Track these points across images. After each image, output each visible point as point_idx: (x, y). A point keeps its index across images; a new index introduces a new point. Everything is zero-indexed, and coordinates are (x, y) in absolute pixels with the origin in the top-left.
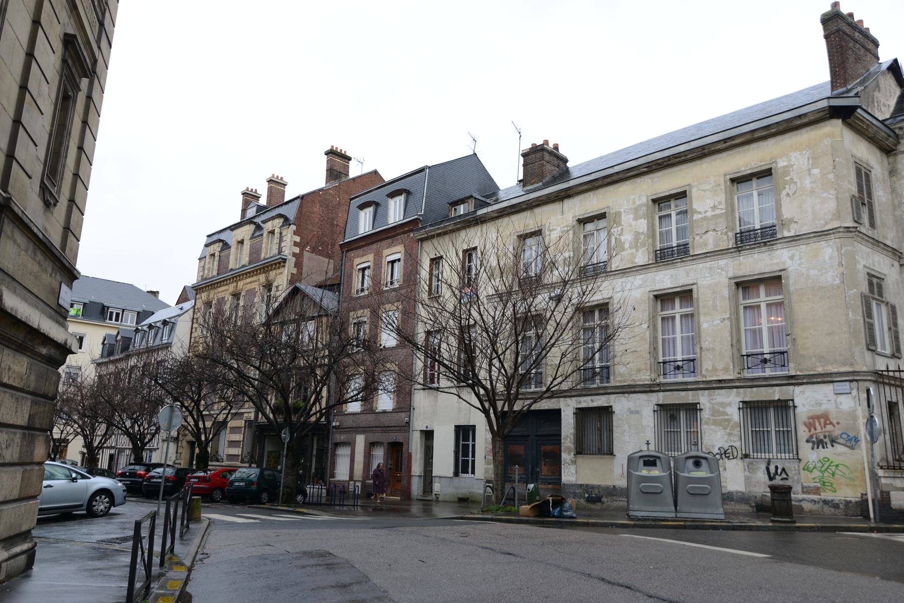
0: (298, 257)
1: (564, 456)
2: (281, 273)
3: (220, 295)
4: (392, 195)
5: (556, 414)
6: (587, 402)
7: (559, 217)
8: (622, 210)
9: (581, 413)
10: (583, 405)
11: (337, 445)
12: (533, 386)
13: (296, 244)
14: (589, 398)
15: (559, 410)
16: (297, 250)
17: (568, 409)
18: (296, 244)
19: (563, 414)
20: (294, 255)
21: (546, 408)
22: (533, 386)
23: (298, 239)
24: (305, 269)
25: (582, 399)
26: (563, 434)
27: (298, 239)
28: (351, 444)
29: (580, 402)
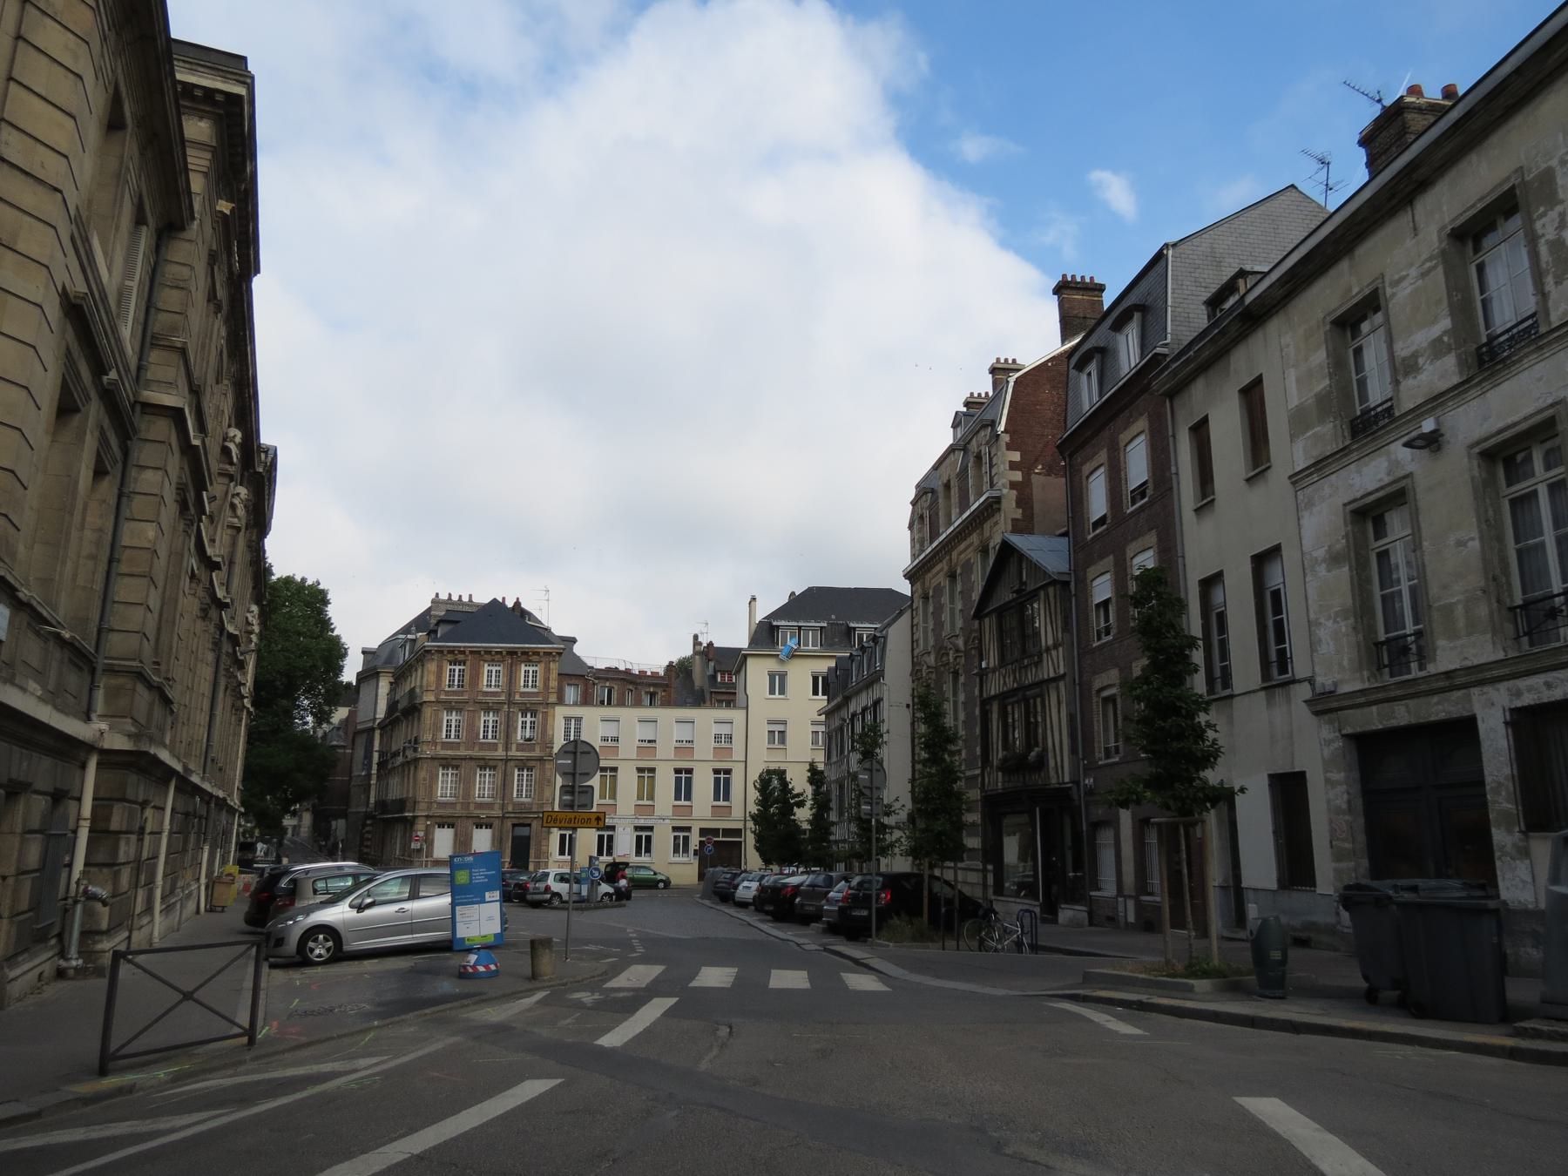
0: (1023, 489)
1: (1499, 836)
2: (996, 523)
3: (935, 582)
4: (1118, 326)
5: (1466, 728)
6: (1536, 690)
7: (1409, 243)
8: (1554, 163)
9: (1525, 722)
10: (1527, 700)
11: (1096, 826)
12: (1414, 666)
13: (1013, 466)
14: (1538, 680)
15: (1472, 721)
16: (1017, 476)
17: (1491, 714)
18: (1013, 466)
19: (1482, 727)
20: (1013, 485)
21: (1442, 716)
22: (1414, 666)
23: (1016, 456)
24: (1037, 507)
25: (1522, 683)
26: (1488, 779)
27: (1016, 456)
28: (1114, 823)
29: (1518, 694)
